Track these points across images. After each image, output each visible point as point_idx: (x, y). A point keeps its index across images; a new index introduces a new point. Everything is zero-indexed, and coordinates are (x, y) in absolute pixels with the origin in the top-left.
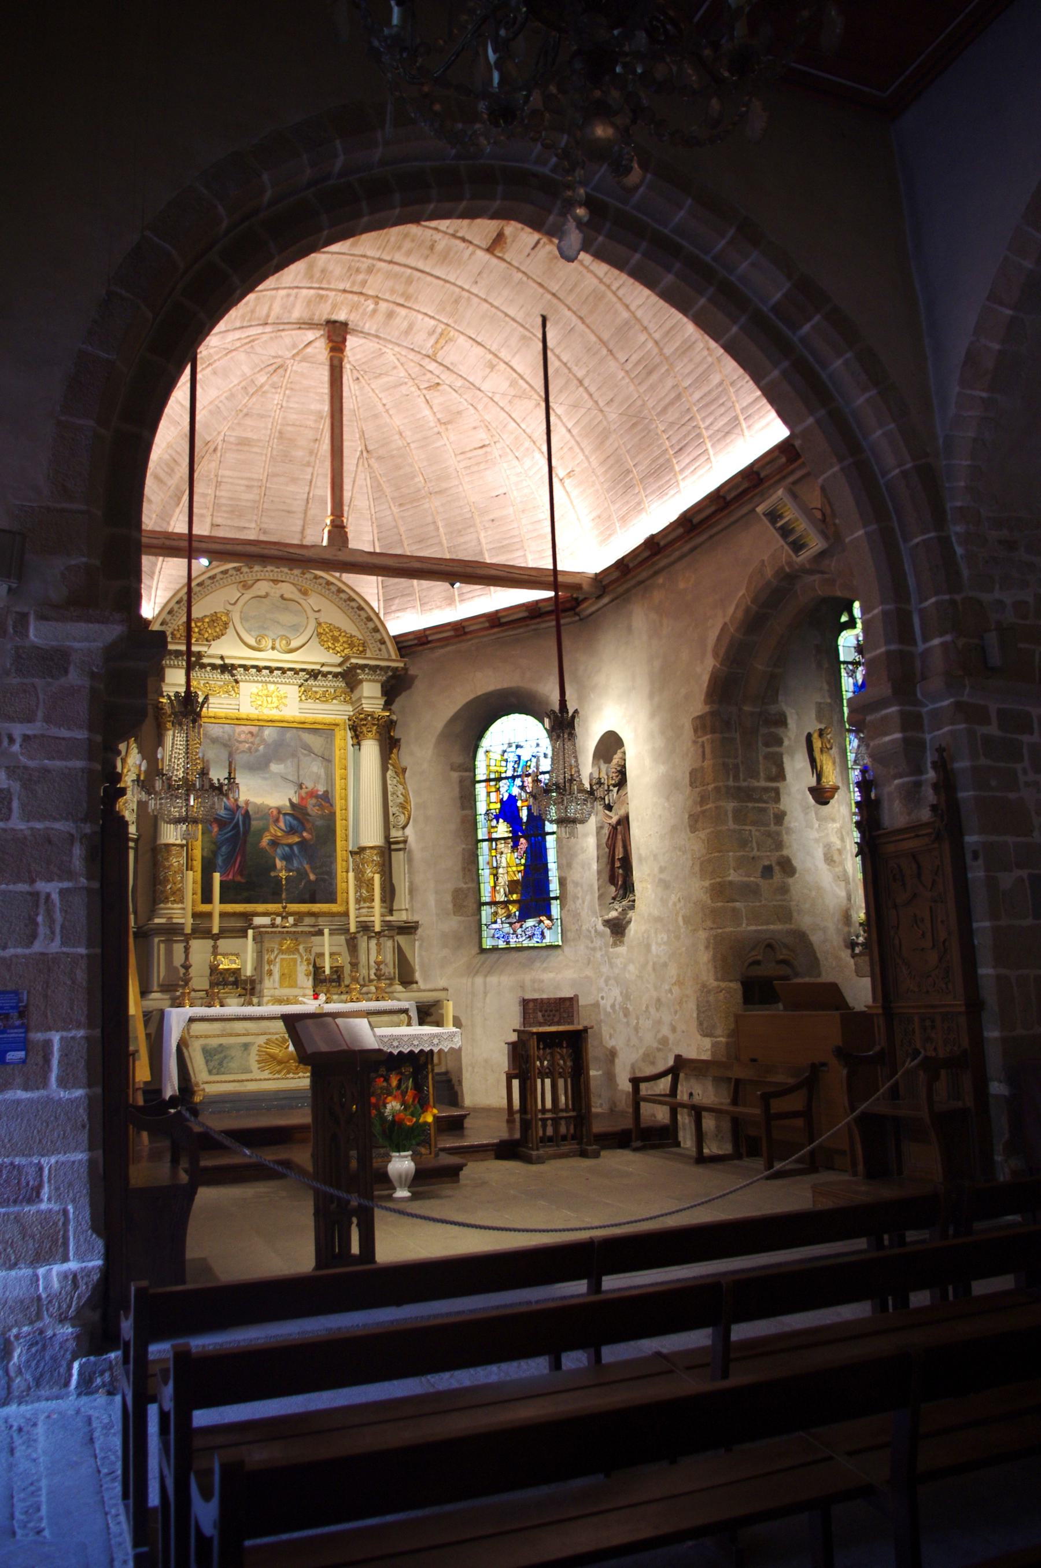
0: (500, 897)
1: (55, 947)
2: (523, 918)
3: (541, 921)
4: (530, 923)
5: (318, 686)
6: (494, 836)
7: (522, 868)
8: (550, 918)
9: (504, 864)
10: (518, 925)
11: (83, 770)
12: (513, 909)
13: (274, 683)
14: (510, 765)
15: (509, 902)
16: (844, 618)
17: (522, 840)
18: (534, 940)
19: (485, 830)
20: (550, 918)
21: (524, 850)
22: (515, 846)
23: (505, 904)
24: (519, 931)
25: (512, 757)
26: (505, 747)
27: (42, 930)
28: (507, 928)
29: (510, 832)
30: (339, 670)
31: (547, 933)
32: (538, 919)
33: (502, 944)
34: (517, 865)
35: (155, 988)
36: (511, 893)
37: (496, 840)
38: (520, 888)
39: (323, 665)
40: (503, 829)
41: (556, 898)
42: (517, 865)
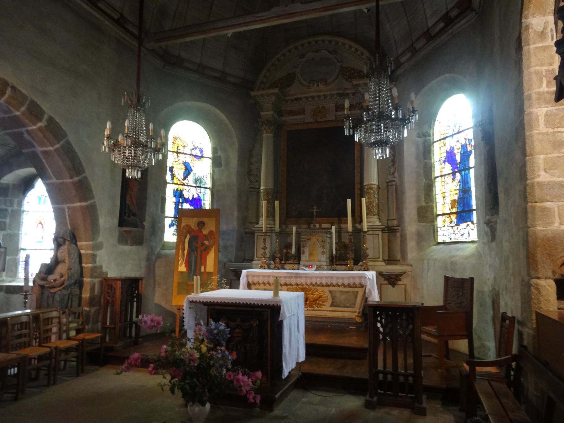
0: (448, 211)
2: (457, 224)
3: (468, 225)
4: (463, 225)
6: (443, 174)
7: (458, 191)
8: (472, 223)
10: (456, 227)
12: (454, 217)
15: (451, 213)
17: (458, 174)
20: (472, 223)
21: (459, 180)
22: (454, 179)
24: (456, 232)
28: (451, 230)
29: (452, 170)
31: (471, 232)
32: (466, 224)
33: (448, 240)
34: (455, 190)
35: (256, 258)
36: (452, 208)
37: (444, 175)
38: (457, 204)
40: (448, 168)
41: (474, 210)
42: (455, 190)
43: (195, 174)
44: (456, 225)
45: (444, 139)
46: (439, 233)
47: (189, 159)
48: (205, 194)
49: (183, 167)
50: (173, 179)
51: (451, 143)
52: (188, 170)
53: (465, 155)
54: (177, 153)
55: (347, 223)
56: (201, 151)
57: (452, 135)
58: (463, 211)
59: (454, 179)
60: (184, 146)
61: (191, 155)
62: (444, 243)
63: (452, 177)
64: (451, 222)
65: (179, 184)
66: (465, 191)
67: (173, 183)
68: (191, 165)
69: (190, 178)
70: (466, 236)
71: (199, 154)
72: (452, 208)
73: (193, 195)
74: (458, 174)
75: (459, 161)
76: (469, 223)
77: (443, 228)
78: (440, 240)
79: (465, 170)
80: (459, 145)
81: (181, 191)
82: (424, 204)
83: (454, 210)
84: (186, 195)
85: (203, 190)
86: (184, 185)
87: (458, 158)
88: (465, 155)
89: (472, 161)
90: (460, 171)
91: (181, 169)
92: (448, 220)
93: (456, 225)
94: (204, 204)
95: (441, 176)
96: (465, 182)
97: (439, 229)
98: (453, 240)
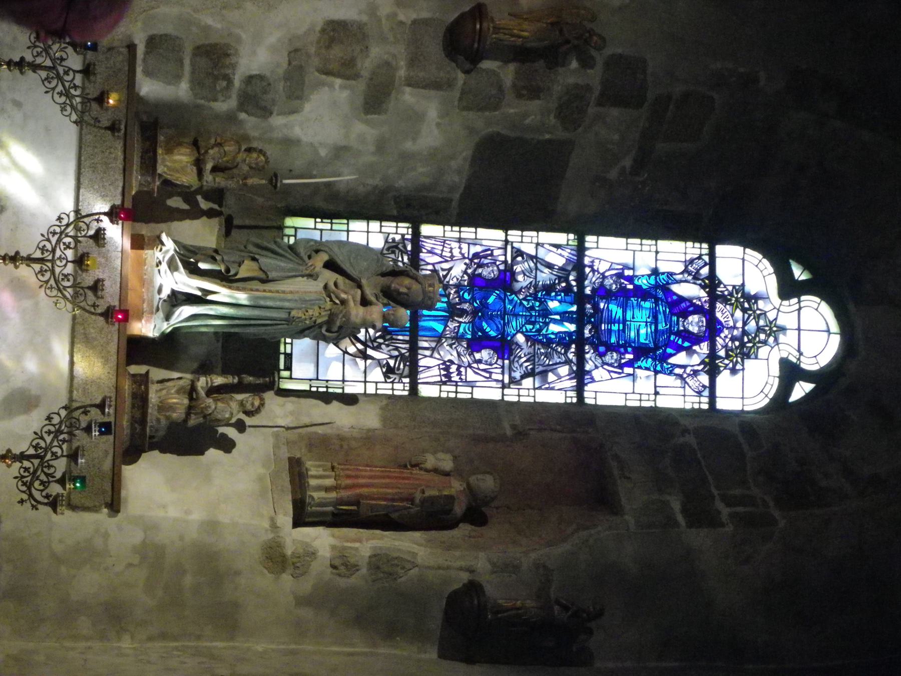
16: (799, 273)
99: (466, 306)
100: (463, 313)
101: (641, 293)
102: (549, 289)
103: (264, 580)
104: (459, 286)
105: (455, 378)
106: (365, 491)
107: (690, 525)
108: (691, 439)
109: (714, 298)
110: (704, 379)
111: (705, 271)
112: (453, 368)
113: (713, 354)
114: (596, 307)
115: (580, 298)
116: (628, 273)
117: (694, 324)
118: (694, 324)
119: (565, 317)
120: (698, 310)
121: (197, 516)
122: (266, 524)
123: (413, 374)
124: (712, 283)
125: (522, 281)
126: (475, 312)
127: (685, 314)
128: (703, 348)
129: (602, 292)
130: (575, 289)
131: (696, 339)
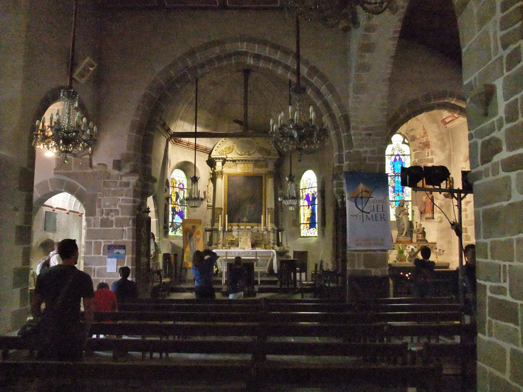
0: (305, 222)
1: (126, 240)
2: (310, 229)
3: (314, 229)
4: (312, 229)
5: (259, 164)
6: (304, 205)
7: (310, 214)
8: (316, 228)
9: (306, 213)
11: (132, 205)
12: (308, 225)
13: (246, 164)
14: (308, 184)
15: (307, 223)
17: (310, 206)
18: (313, 234)
19: (302, 203)
20: (316, 228)
22: (309, 208)
23: (306, 224)
24: (309, 232)
25: (309, 183)
26: (307, 180)
27: (124, 236)
28: (307, 231)
30: (263, 159)
31: (315, 232)
32: (313, 229)
33: (305, 236)
36: (308, 221)
39: (259, 158)
40: (306, 203)
43: (180, 198)
44: (309, 229)
45: (305, 189)
46: (301, 232)
47: (178, 191)
48: (184, 209)
49: (175, 195)
50: (171, 202)
51: (308, 191)
52: (178, 196)
53: (314, 199)
54: (173, 187)
55: (261, 226)
56: (183, 185)
57: (309, 188)
58: (312, 223)
59: (309, 208)
60: (176, 183)
61: (178, 188)
62: (304, 237)
63: (308, 207)
64: (307, 227)
65: (174, 204)
66: (313, 214)
67: (172, 204)
68: (179, 193)
69: (178, 200)
70: (313, 234)
71: (182, 187)
72: (308, 221)
73: (180, 210)
74: (310, 206)
75: (311, 200)
76: (314, 228)
77: (303, 230)
78: (302, 235)
79: (313, 205)
80: (311, 194)
81: (175, 208)
82: (295, 218)
83: (308, 222)
84: (177, 210)
85: (183, 207)
86: (175, 205)
87: (311, 199)
88: (314, 199)
89: (316, 202)
90: (311, 205)
91: (175, 196)
92: (305, 226)
93: (309, 229)
94: (184, 215)
95: (303, 206)
96: (313, 210)
97: (301, 230)
98: (307, 236)
99: (398, 193)
100: (399, 194)
101: (394, 166)
102: (394, 181)
103: (443, 223)
104: (395, 194)
105: (408, 195)
106: (430, 209)
107: (433, 162)
108: (417, 160)
109: (393, 155)
110: (405, 156)
111: (390, 156)
112: (407, 195)
113: (402, 155)
114: (397, 173)
115: (395, 176)
116: (391, 168)
117: (397, 158)
118: (397, 158)
119: (398, 178)
120: (395, 157)
121: (436, 232)
122: (436, 223)
123: (408, 201)
124: (391, 155)
125: (393, 185)
126: (398, 192)
127: (396, 159)
128: (401, 156)
129: (394, 172)
130: (394, 177)
131: (400, 158)
